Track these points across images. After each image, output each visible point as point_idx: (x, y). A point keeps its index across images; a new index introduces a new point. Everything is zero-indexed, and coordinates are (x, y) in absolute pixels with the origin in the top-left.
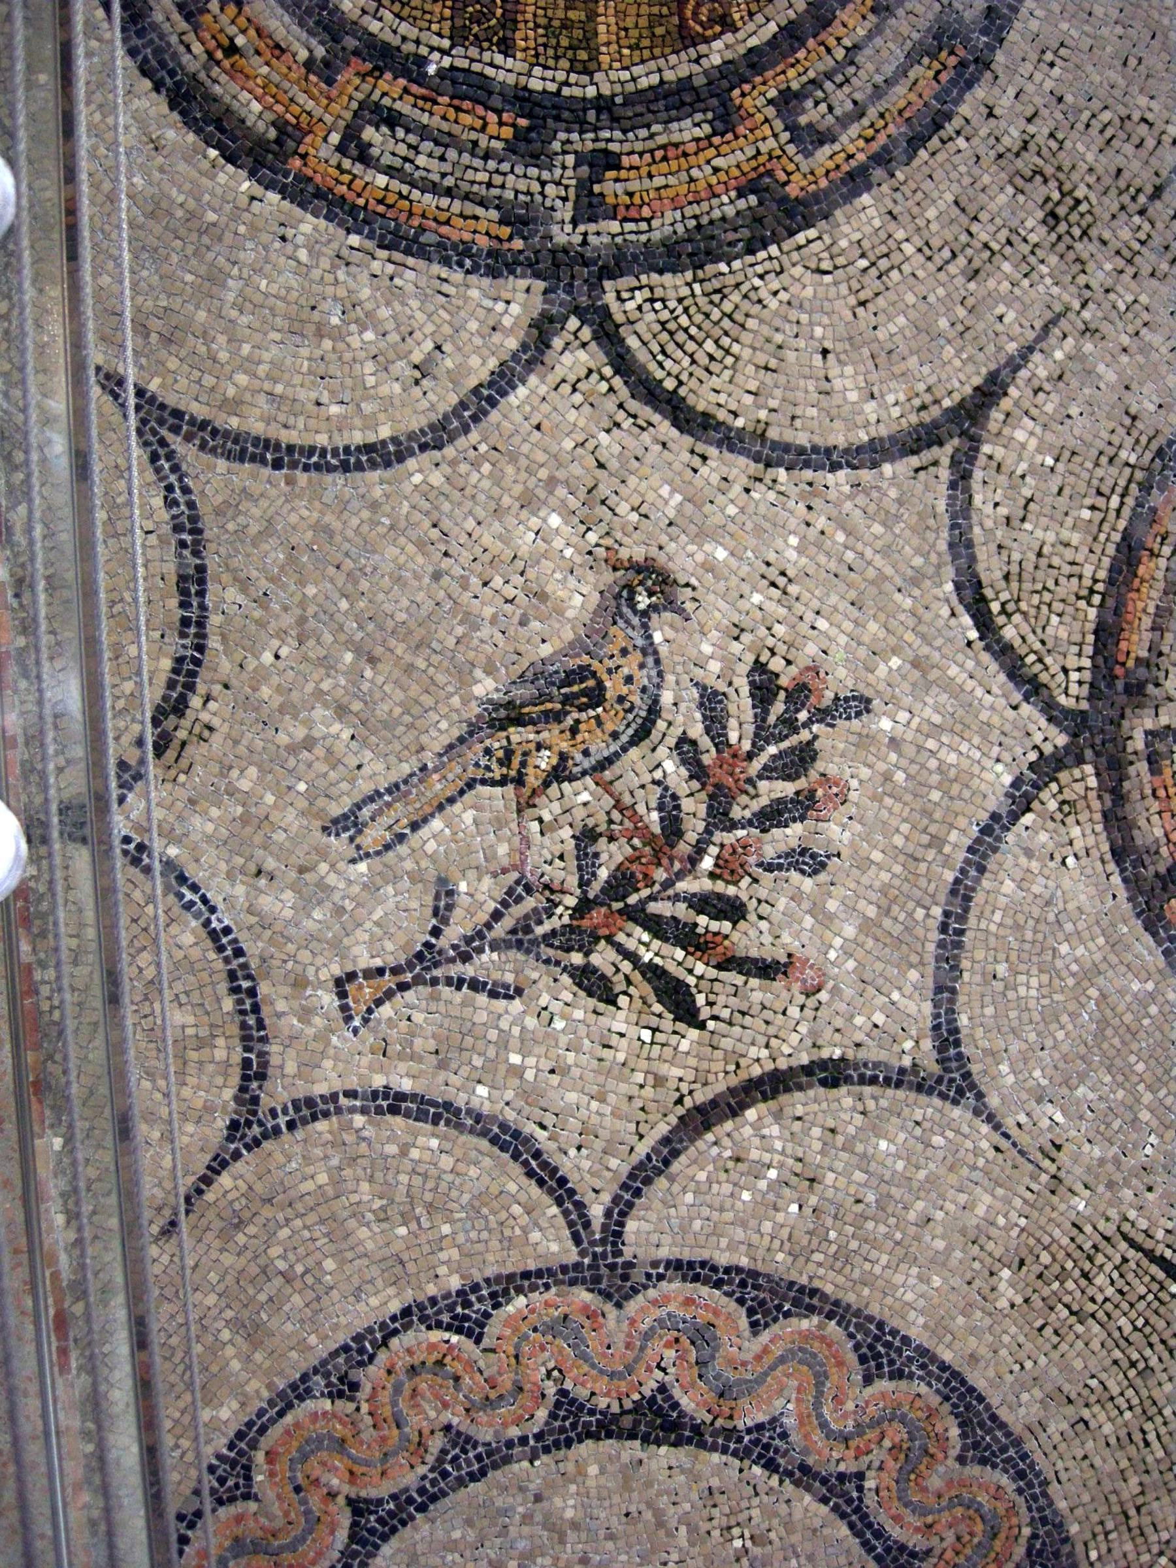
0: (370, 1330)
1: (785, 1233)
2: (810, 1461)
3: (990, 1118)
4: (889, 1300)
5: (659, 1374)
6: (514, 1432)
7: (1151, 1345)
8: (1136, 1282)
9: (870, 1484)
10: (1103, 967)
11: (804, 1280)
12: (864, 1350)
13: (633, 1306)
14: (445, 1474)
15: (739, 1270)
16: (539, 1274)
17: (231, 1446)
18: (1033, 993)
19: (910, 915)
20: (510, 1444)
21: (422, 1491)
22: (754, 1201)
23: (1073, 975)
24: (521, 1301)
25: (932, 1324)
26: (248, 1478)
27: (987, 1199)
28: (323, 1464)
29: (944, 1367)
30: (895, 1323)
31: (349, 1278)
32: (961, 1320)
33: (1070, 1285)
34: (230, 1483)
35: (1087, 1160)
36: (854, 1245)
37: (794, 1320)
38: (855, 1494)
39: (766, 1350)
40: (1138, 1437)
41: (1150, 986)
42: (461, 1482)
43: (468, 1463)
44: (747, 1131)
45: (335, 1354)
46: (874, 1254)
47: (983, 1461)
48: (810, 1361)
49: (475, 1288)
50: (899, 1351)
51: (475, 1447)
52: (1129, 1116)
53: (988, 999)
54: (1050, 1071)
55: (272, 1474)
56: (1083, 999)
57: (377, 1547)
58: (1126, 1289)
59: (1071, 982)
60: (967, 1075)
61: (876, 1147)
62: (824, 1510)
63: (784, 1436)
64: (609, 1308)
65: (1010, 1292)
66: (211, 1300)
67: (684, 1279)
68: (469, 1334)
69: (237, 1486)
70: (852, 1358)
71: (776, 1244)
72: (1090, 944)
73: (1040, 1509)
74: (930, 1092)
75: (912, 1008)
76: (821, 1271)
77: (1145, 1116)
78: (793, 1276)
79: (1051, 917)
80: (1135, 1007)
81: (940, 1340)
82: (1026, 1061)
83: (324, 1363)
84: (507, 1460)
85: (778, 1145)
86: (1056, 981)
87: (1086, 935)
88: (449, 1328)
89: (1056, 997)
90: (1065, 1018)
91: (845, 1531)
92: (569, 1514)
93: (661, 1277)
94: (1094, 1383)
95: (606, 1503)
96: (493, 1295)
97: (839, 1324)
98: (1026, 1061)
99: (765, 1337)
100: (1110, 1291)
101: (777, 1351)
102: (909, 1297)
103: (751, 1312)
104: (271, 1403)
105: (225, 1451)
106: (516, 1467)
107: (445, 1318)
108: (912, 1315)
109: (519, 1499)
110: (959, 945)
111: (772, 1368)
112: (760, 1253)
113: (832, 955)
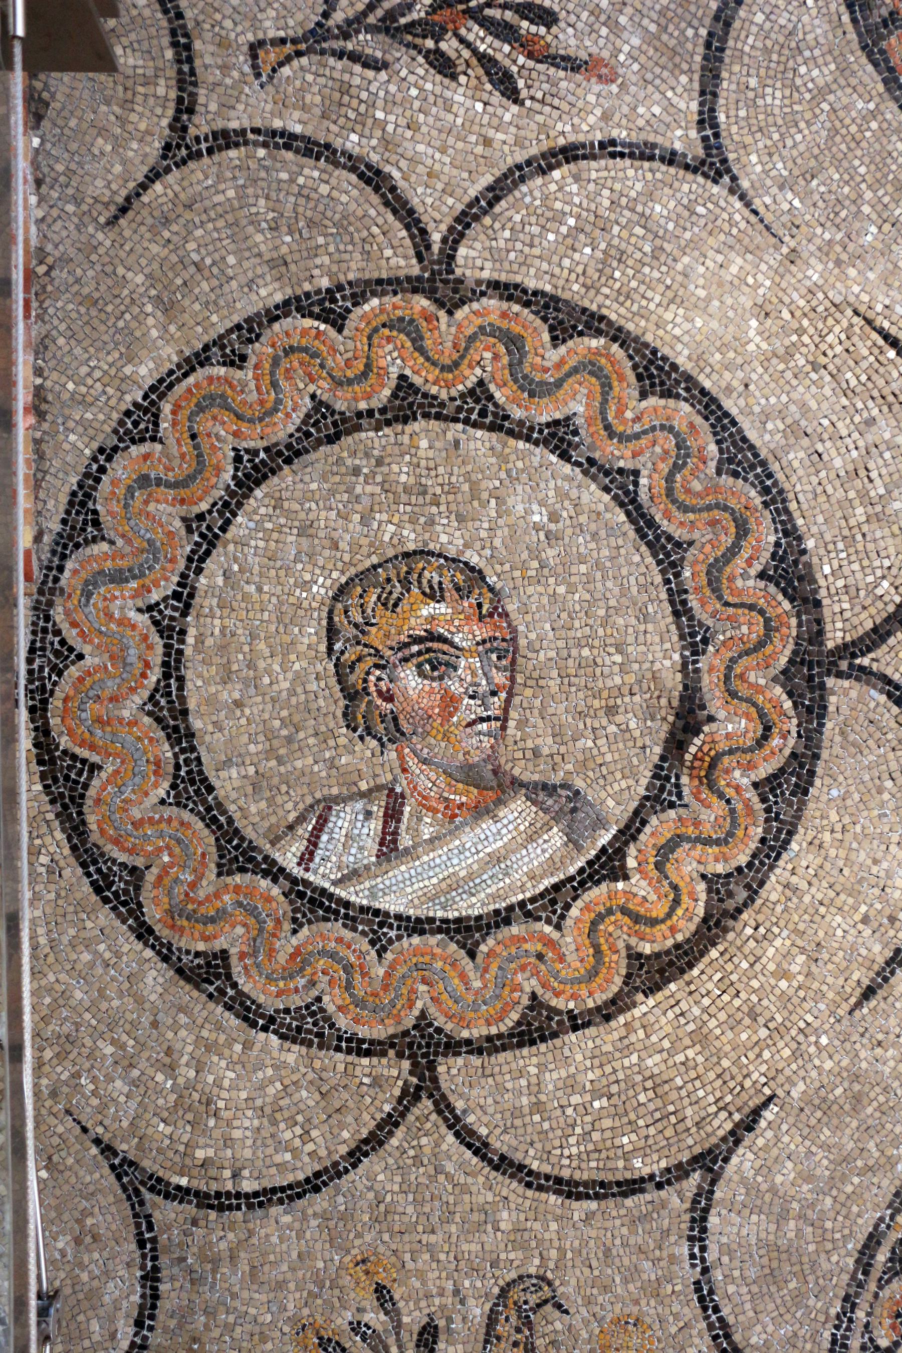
0: (258, 314)
1: (580, 269)
2: (597, 455)
3: (742, 197)
4: (661, 332)
5: (478, 371)
6: (363, 406)
7: (873, 398)
8: (860, 344)
9: (643, 481)
10: (834, 87)
11: (594, 307)
12: (641, 370)
13: (460, 314)
14: (308, 435)
15: (544, 294)
16: (389, 282)
17: (145, 397)
18: (777, 102)
19: (683, 32)
20: (359, 415)
21: (289, 446)
22: (556, 241)
23: (810, 91)
24: (375, 302)
25: (695, 357)
26: (156, 424)
27: (739, 261)
28: (214, 418)
29: (703, 392)
30: (665, 351)
31: (245, 272)
32: (718, 356)
33: (806, 339)
34: (142, 426)
35: (818, 241)
36: (634, 284)
37: (586, 339)
38: (631, 487)
39: (562, 362)
40: (862, 473)
41: (872, 106)
42: (319, 443)
43: (327, 428)
44: (553, 187)
45: (230, 331)
46: (649, 294)
47: (735, 475)
48: (597, 372)
49: (340, 288)
50: (668, 374)
51: (332, 415)
52: (853, 208)
53: (741, 104)
54: (790, 164)
55: (174, 424)
56: (817, 111)
57: (251, 490)
58: (852, 349)
59: (808, 96)
60: (724, 161)
61: (653, 209)
62: (607, 498)
63: (575, 433)
64: (442, 314)
65: (758, 339)
66: (140, 279)
67: (501, 298)
68: (333, 325)
69: (147, 430)
70: (631, 377)
71: (573, 276)
72: (824, 69)
73: (782, 522)
74: (695, 171)
75: (682, 105)
76: (608, 302)
77: (866, 209)
78: (586, 303)
79: (793, 45)
80: (859, 121)
81: (702, 370)
82: (770, 155)
83: (221, 337)
84: (358, 428)
85: (576, 200)
86: (796, 95)
87: (820, 61)
88: (317, 318)
89: (796, 108)
90: (802, 125)
91: (623, 517)
92: (403, 478)
93: (483, 294)
94: (826, 422)
95: (433, 473)
96: (353, 296)
97: (621, 346)
98: (770, 155)
99: (563, 350)
100: (839, 349)
101: (572, 362)
102: (677, 332)
103: (552, 329)
104: (179, 366)
105: (140, 400)
106: (363, 435)
107: (316, 309)
108: (679, 347)
109: (364, 462)
110: (721, 60)
111: (569, 375)
112: (561, 283)
113: (622, 58)
